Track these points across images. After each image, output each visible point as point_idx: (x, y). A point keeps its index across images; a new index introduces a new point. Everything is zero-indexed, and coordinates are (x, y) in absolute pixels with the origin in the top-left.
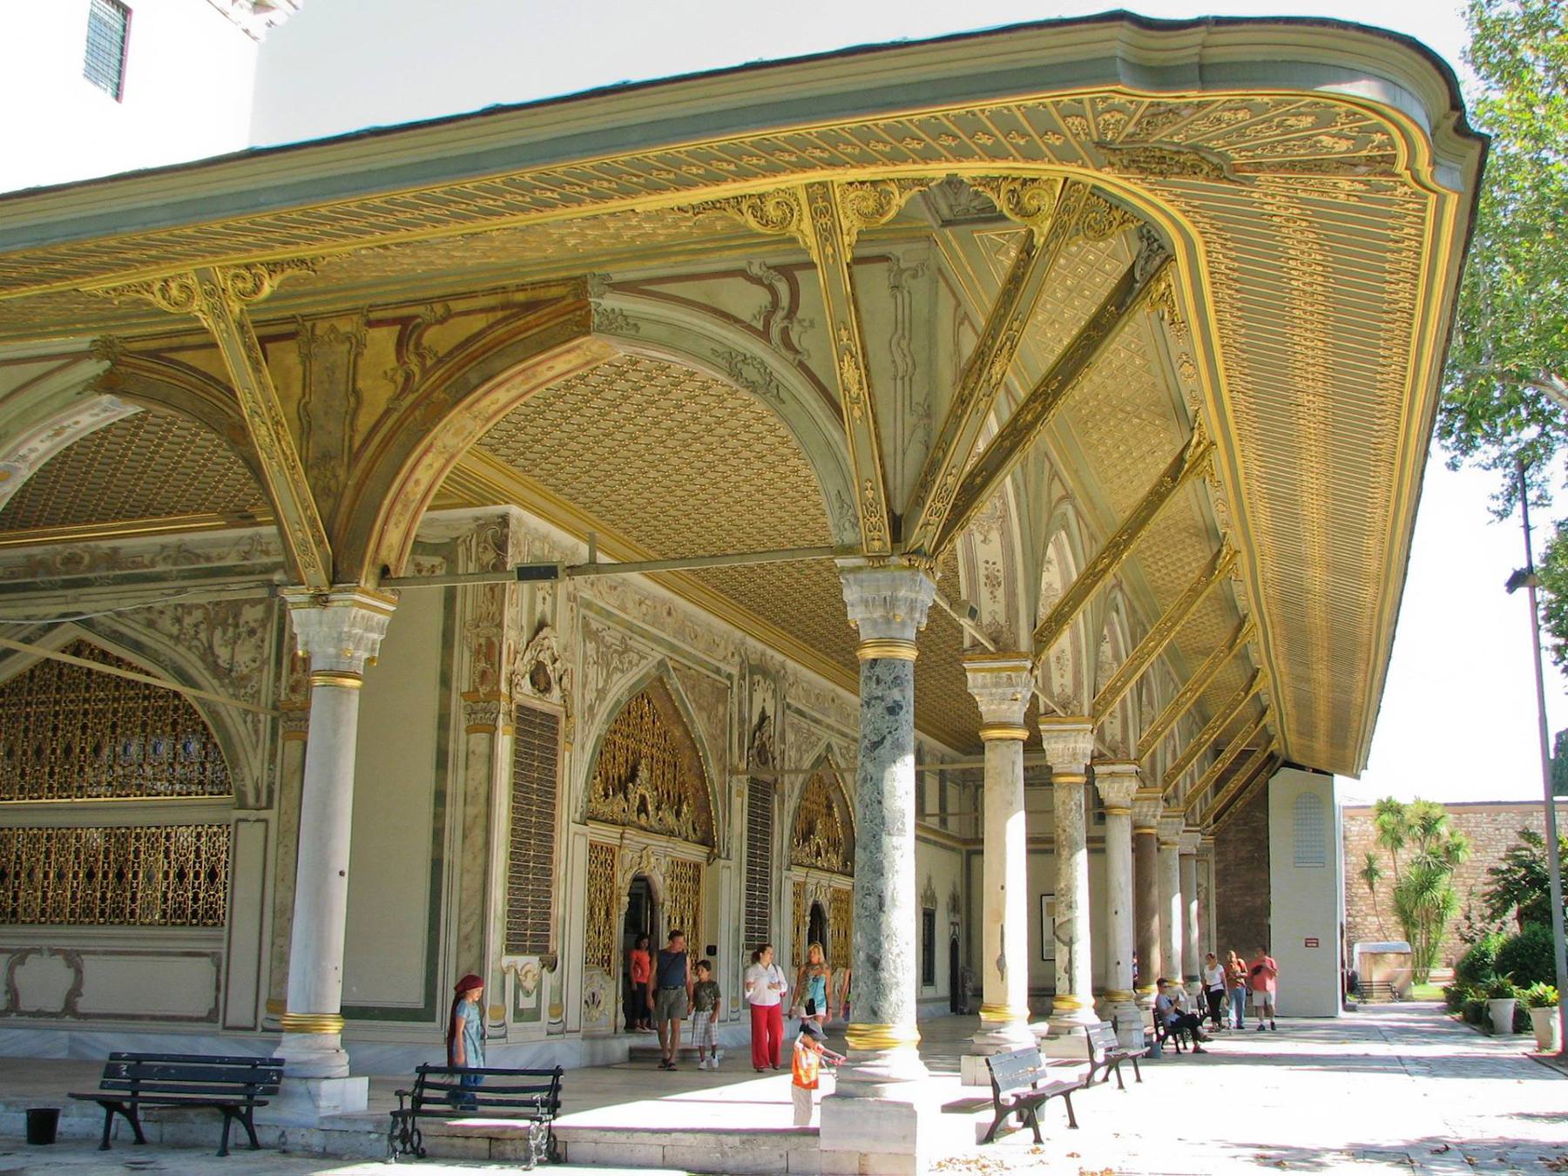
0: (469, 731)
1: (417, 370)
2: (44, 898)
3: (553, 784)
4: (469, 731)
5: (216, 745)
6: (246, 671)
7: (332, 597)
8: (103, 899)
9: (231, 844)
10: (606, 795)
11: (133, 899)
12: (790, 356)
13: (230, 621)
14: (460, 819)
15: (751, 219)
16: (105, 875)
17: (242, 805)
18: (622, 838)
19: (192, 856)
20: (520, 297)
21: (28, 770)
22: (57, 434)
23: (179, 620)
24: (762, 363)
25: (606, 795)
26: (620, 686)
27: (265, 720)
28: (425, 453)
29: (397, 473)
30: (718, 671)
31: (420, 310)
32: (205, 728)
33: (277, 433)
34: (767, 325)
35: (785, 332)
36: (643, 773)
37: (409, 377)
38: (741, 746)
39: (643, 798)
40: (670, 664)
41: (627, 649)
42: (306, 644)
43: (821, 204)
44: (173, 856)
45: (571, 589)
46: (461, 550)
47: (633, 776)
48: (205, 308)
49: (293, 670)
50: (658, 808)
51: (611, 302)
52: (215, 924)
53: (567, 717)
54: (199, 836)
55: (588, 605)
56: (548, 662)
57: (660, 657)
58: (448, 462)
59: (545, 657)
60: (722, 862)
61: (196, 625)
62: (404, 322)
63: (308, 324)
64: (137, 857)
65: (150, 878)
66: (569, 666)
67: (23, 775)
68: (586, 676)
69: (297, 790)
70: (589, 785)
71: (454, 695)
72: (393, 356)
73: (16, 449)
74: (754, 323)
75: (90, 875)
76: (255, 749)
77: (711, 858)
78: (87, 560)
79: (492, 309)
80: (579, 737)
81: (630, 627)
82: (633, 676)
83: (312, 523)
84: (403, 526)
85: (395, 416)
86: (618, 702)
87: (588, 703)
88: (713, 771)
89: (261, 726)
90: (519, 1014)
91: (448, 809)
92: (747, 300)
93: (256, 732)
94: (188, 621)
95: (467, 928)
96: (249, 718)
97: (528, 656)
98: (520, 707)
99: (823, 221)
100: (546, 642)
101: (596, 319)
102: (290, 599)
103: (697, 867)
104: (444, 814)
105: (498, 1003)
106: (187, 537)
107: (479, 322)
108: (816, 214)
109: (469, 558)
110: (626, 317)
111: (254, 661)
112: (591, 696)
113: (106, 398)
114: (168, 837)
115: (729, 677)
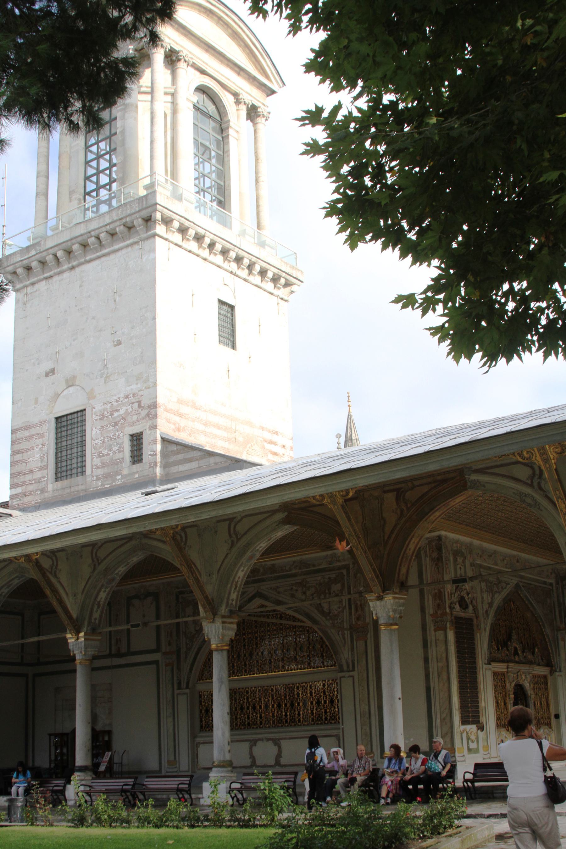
0: (435, 630)
1: (405, 508)
2: (261, 717)
3: (474, 649)
4: (435, 630)
5: (327, 646)
6: (336, 613)
7: (384, 596)
8: (286, 715)
9: (339, 687)
10: (498, 649)
11: (299, 715)
12: (541, 492)
13: (327, 591)
14: (436, 669)
15: (518, 457)
16: (286, 705)
17: (342, 671)
18: (508, 668)
19: (322, 694)
20: (439, 478)
21: (247, 663)
22: (269, 540)
23: (304, 593)
24: (532, 496)
25: (498, 649)
26: (498, 599)
27: (347, 633)
28: (411, 539)
29: (403, 548)
30: (545, 583)
31: (403, 485)
32: (321, 638)
33: (359, 541)
34: (532, 482)
35: (539, 484)
36: (514, 637)
37: (402, 511)
38: (561, 617)
39: (516, 649)
40: (521, 584)
41: (500, 582)
42: (376, 614)
43: (542, 451)
44: (314, 695)
45: (471, 561)
46: (422, 552)
47: (510, 638)
48: (329, 501)
49: (356, 610)
50: (523, 652)
51: (474, 477)
52: (335, 723)
53: (477, 618)
54: (324, 685)
55: (480, 566)
56: (465, 596)
57: (515, 582)
58: (420, 540)
59: (464, 594)
60: (557, 674)
61: (312, 595)
62: (398, 490)
63: (362, 494)
64: (298, 696)
65: (305, 704)
66: (475, 595)
67: (245, 665)
68: (483, 598)
69: (364, 662)
70: (490, 646)
71: (427, 616)
72: (395, 504)
73: (256, 547)
74: (527, 481)
75: (279, 706)
76: (344, 646)
77: (552, 672)
78: (262, 570)
79: (430, 483)
80: (483, 626)
81: (500, 572)
82: (504, 593)
83: (374, 570)
84: (406, 566)
85: (399, 526)
86: (498, 608)
87: (485, 610)
88: (548, 631)
89: (346, 636)
90: (470, 750)
91: (430, 665)
92: (523, 473)
93: (344, 638)
94: (308, 593)
95: (444, 715)
96: (340, 633)
97: (456, 595)
98: (456, 618)
99: (544, 456)
100: (463, 587)
101: (469, 484)
102: (368, 598)
103: (545, 677)
104: (429, 667)
105: (461, 746)
106: (304, 557)
107: (426, 489)
108: (541, 455)
109: (426, 556)
110: (480, 482)
111: (339, 608)
112: (486, 606)
113: (287, 527)
114: (311, 687)
115: (551, 584)
